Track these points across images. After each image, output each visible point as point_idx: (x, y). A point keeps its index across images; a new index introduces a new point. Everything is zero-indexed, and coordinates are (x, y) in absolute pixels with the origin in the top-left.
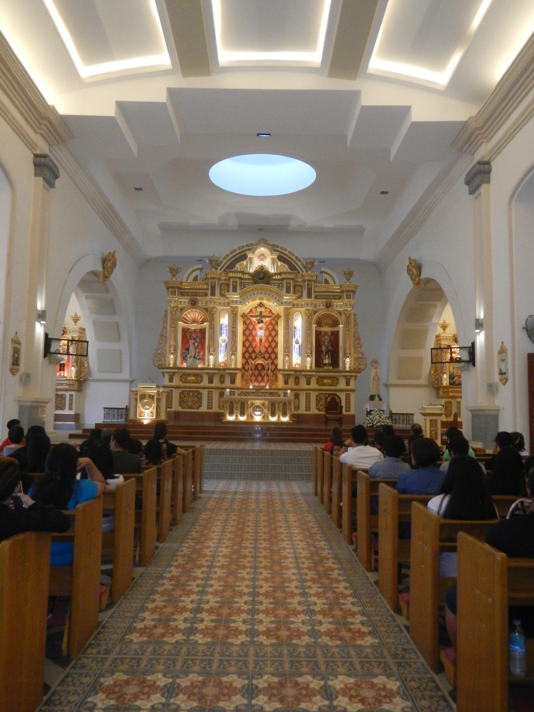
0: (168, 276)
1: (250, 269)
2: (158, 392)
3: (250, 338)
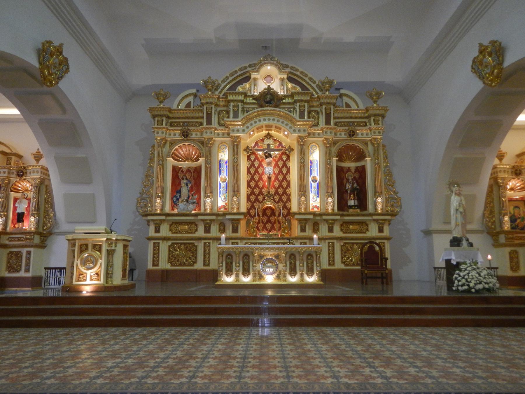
0: (155, 104)
1: (254, 92)
2: (107, 239)
3: (257, 177)
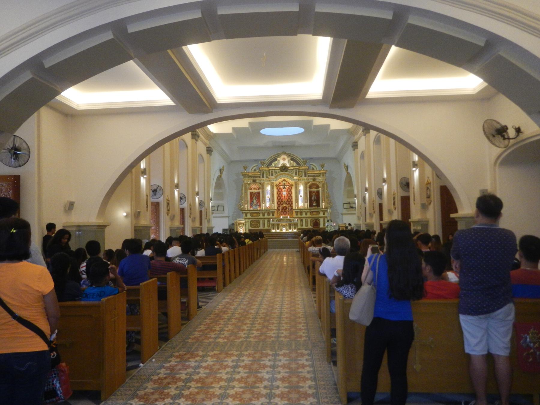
0: (242, 170)
3: (280, 195)
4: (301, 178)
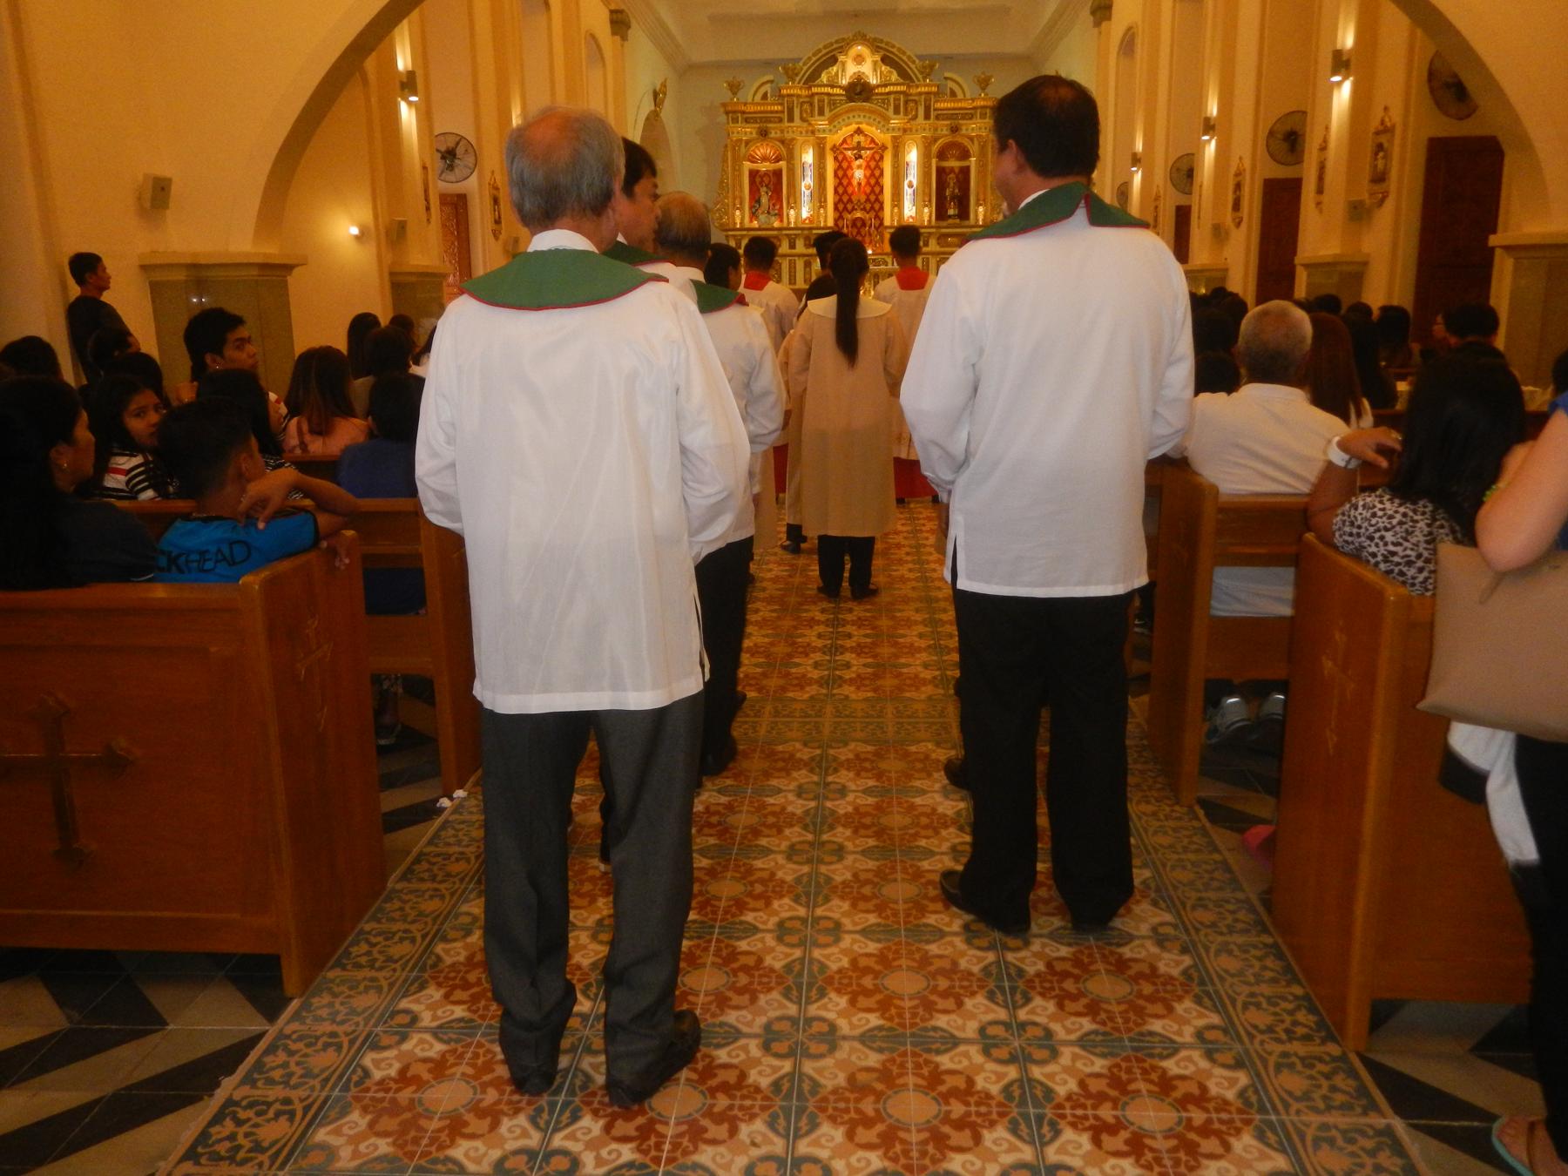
0: (726, 96)
3: (845, 182)
4: (912, 122)
